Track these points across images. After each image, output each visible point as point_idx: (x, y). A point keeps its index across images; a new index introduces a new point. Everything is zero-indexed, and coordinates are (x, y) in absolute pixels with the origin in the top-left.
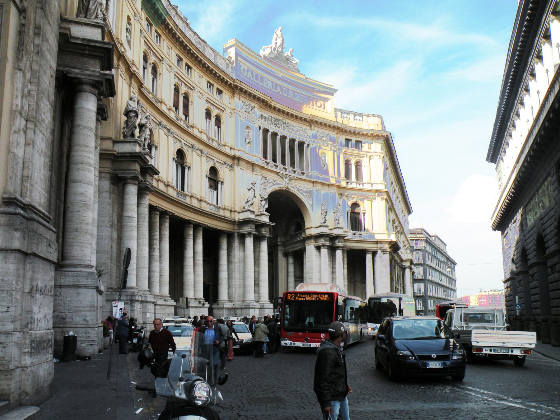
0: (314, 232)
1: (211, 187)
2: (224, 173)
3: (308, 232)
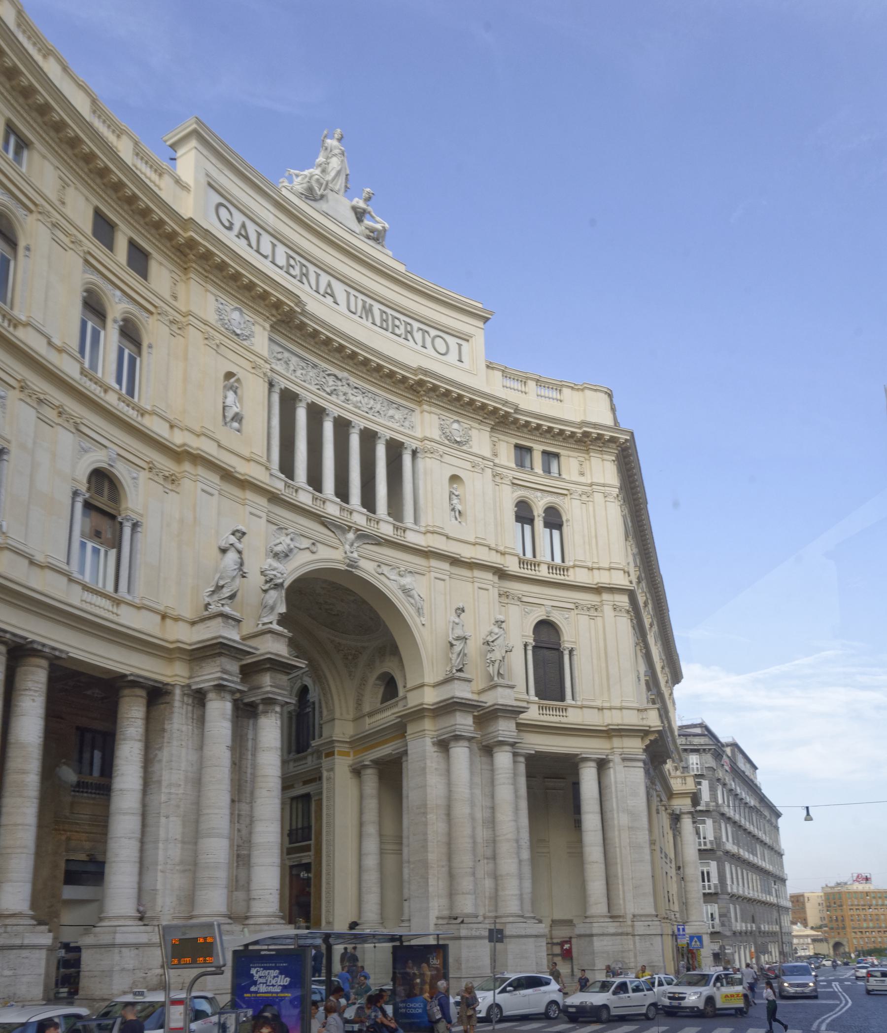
0: (430, 697)
3: (413, 700)
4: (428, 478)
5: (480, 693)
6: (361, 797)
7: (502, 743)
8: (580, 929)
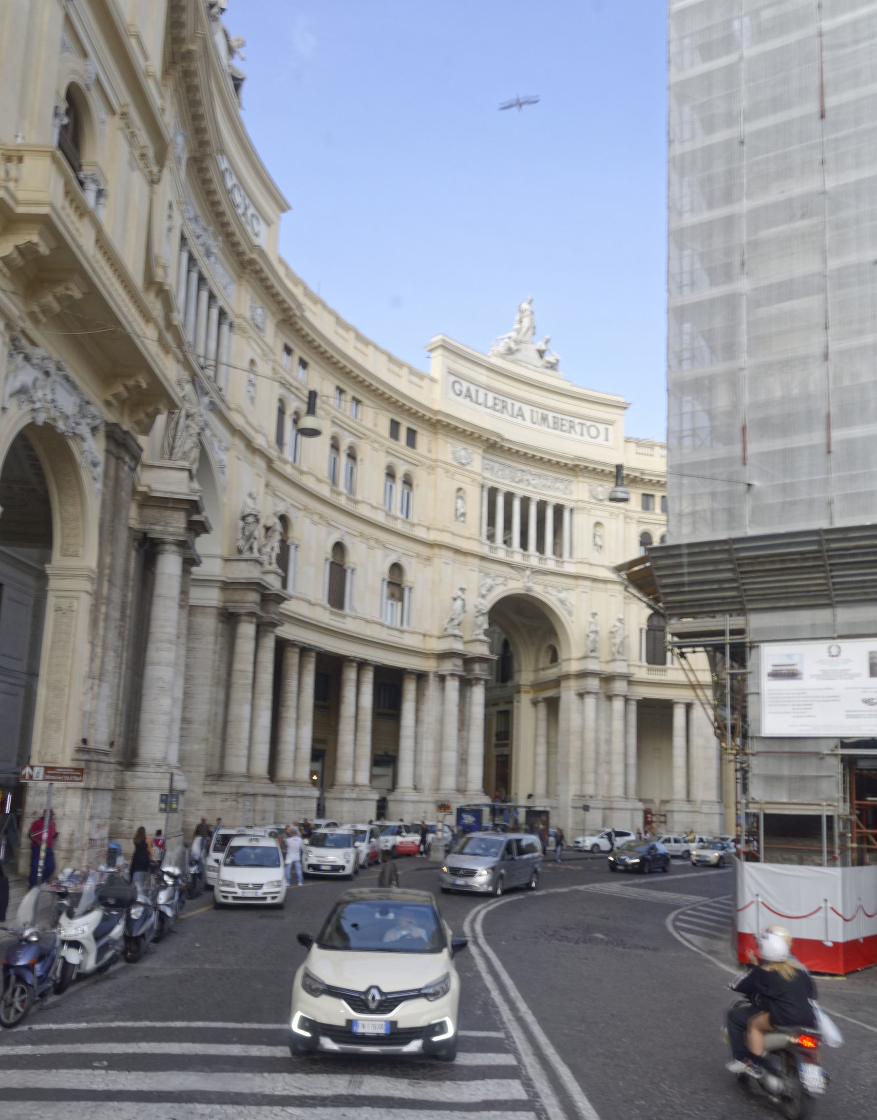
0: (574, 667)
1: (392, 596)
2: (413, 574)
4: (579, 527)
5: (608, 662)
6: (537, 720)
7: (617, 695)
8: (668, 807)
